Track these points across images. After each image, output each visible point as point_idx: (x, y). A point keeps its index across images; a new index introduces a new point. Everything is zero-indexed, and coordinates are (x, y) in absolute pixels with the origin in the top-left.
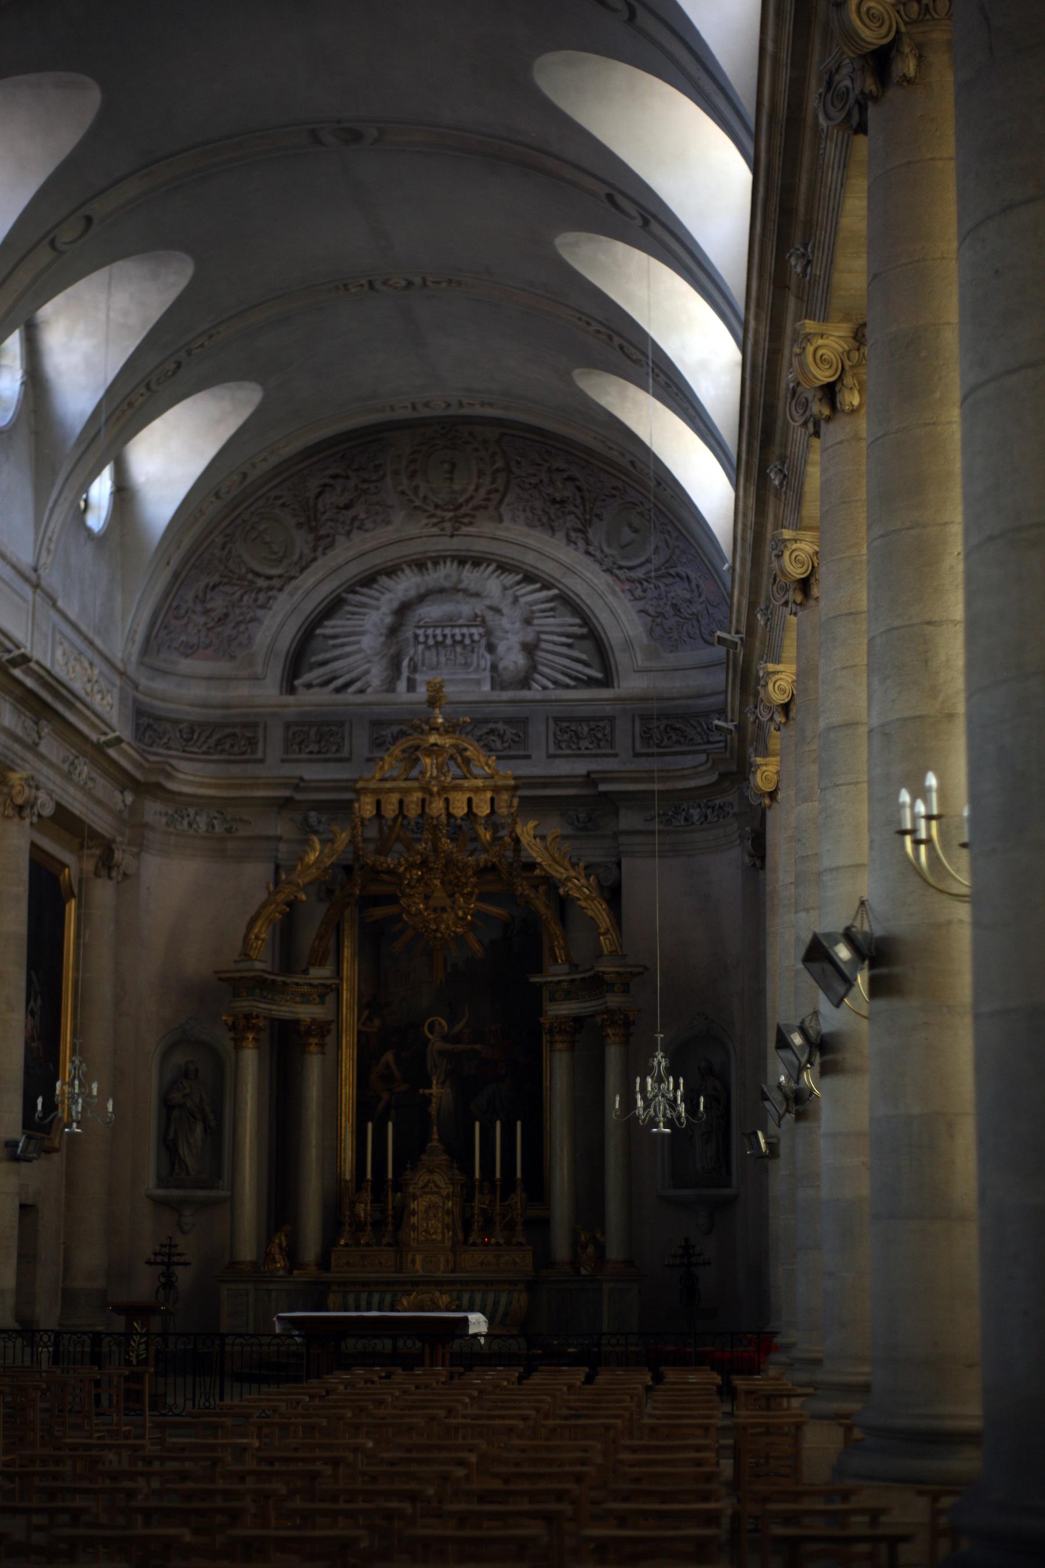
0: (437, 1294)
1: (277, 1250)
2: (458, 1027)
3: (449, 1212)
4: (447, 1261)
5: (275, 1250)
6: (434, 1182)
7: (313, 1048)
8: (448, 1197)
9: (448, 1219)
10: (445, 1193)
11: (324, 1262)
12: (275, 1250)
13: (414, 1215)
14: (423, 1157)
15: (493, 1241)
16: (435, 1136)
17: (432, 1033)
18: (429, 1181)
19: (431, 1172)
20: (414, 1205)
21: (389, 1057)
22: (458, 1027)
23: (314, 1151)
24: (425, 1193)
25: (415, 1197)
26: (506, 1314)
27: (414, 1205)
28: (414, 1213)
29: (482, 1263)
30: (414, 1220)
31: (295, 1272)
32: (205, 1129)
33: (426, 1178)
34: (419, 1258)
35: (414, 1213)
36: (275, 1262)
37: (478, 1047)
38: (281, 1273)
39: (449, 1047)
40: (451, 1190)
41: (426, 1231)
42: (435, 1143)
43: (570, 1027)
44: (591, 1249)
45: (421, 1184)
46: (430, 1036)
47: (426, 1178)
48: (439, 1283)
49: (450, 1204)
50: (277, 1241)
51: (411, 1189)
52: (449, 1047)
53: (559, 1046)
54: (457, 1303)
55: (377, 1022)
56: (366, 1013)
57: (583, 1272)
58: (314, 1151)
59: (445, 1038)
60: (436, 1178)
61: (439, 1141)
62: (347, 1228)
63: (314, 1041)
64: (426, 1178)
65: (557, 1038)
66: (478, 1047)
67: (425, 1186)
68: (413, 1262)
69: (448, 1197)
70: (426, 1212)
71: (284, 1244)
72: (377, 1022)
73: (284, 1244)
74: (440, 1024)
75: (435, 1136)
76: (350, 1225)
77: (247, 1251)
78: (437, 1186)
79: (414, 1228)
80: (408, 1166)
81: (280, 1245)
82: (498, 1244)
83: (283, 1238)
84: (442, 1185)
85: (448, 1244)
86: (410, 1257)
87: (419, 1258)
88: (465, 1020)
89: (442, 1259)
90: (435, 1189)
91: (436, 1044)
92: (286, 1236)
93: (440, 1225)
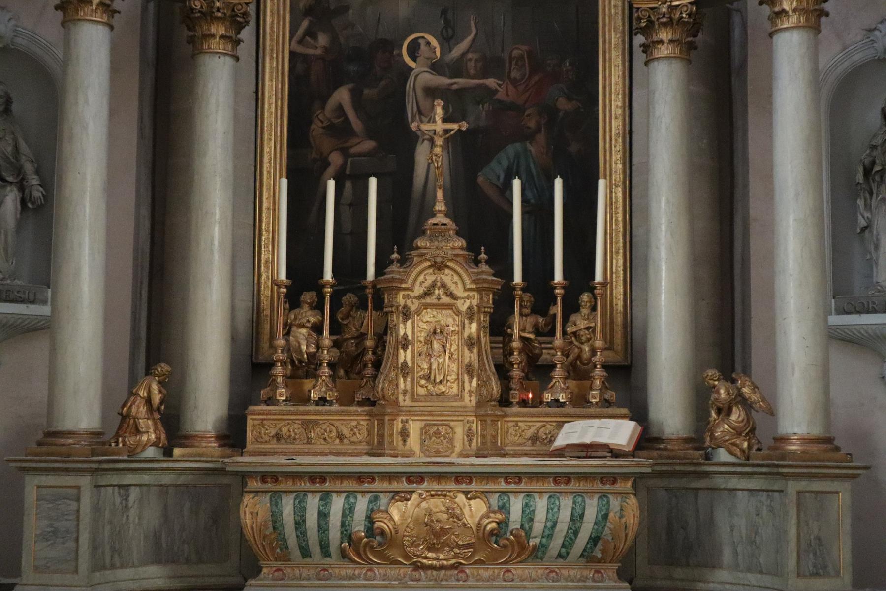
0: (461, 498)
1: (143, 410)
2: (457, 52)
3: (471, 343)
4: (469, 435)
5: (140, 410)
6: (443, 286)
7: (216, 45)
8: (470, 315)
9: (471, 356)
10: (463, 306)
11: (233, 434)
12: (140, 410)
13: (405, 347)
14: (420, 242)
15: (548, 397)
16: (440, 206)
17: (414, 59)
18: (434, 285)
19: (439, 267)
20: (405, 329)
21: (342, 96)
22: (456, 52)
23: (216, 231)
24: (426, 306)
25: (407, 314)
26: (594, 540)
27: (405, 329)
28: (405, 343)
29: (534, 439)
30: (405, 356)
31: (177, 451)
32: (23, 202)
33: (430, 278)
34: (415, 428)
35: (405, 343)
36: (137, 431)
37: (491, 82)
38: (150, 452)
39: (444, 81)
40: (475, 302)
41: (428, 378)
42: (440, 219)
43: (690, 15)
44: (736, 415)
45: (418, 290)
46: (412, 64)
47: (430, 279)
48: (460, 477)
49: (474, 326)
50: (143, 393)
51: (400, 299)
52: (444, 81)
53: (664, 51)
54: (499, 516)
55: (323, 40)
56: (305, 24)
57: (723, 455)
58: (216, 231)
59: (436, 67)
60: (448, 277)
61: (446, 215)
62: (278, 370)
63: (219, 30)
64: (430, 278)
65: (665, 35)
66: (491, 82)
67: (427, 294)
68: (404, 434)
69: (470, 315)
70: (428, 342)
71: (157, 398)
72: (323, 40)
73: (157, 398)
74: (428, 43)
75: (440, 206)
76: (284, 364)
77: (82, 412)
78: (451, 295)
79: (405, 370)
80: (395, 256)
81: (148, 401)
82: (556, 403)
83: (155, 387)
84: (459, 292)
85: (470, 401)
86: (398, 425)
87: (415, 428)
88: (470, 38)
89: (460, 431)
90: (445, 300)
91: (421, 76)
92: (160, 382)
93: (454, 367)
